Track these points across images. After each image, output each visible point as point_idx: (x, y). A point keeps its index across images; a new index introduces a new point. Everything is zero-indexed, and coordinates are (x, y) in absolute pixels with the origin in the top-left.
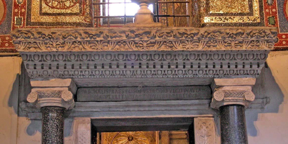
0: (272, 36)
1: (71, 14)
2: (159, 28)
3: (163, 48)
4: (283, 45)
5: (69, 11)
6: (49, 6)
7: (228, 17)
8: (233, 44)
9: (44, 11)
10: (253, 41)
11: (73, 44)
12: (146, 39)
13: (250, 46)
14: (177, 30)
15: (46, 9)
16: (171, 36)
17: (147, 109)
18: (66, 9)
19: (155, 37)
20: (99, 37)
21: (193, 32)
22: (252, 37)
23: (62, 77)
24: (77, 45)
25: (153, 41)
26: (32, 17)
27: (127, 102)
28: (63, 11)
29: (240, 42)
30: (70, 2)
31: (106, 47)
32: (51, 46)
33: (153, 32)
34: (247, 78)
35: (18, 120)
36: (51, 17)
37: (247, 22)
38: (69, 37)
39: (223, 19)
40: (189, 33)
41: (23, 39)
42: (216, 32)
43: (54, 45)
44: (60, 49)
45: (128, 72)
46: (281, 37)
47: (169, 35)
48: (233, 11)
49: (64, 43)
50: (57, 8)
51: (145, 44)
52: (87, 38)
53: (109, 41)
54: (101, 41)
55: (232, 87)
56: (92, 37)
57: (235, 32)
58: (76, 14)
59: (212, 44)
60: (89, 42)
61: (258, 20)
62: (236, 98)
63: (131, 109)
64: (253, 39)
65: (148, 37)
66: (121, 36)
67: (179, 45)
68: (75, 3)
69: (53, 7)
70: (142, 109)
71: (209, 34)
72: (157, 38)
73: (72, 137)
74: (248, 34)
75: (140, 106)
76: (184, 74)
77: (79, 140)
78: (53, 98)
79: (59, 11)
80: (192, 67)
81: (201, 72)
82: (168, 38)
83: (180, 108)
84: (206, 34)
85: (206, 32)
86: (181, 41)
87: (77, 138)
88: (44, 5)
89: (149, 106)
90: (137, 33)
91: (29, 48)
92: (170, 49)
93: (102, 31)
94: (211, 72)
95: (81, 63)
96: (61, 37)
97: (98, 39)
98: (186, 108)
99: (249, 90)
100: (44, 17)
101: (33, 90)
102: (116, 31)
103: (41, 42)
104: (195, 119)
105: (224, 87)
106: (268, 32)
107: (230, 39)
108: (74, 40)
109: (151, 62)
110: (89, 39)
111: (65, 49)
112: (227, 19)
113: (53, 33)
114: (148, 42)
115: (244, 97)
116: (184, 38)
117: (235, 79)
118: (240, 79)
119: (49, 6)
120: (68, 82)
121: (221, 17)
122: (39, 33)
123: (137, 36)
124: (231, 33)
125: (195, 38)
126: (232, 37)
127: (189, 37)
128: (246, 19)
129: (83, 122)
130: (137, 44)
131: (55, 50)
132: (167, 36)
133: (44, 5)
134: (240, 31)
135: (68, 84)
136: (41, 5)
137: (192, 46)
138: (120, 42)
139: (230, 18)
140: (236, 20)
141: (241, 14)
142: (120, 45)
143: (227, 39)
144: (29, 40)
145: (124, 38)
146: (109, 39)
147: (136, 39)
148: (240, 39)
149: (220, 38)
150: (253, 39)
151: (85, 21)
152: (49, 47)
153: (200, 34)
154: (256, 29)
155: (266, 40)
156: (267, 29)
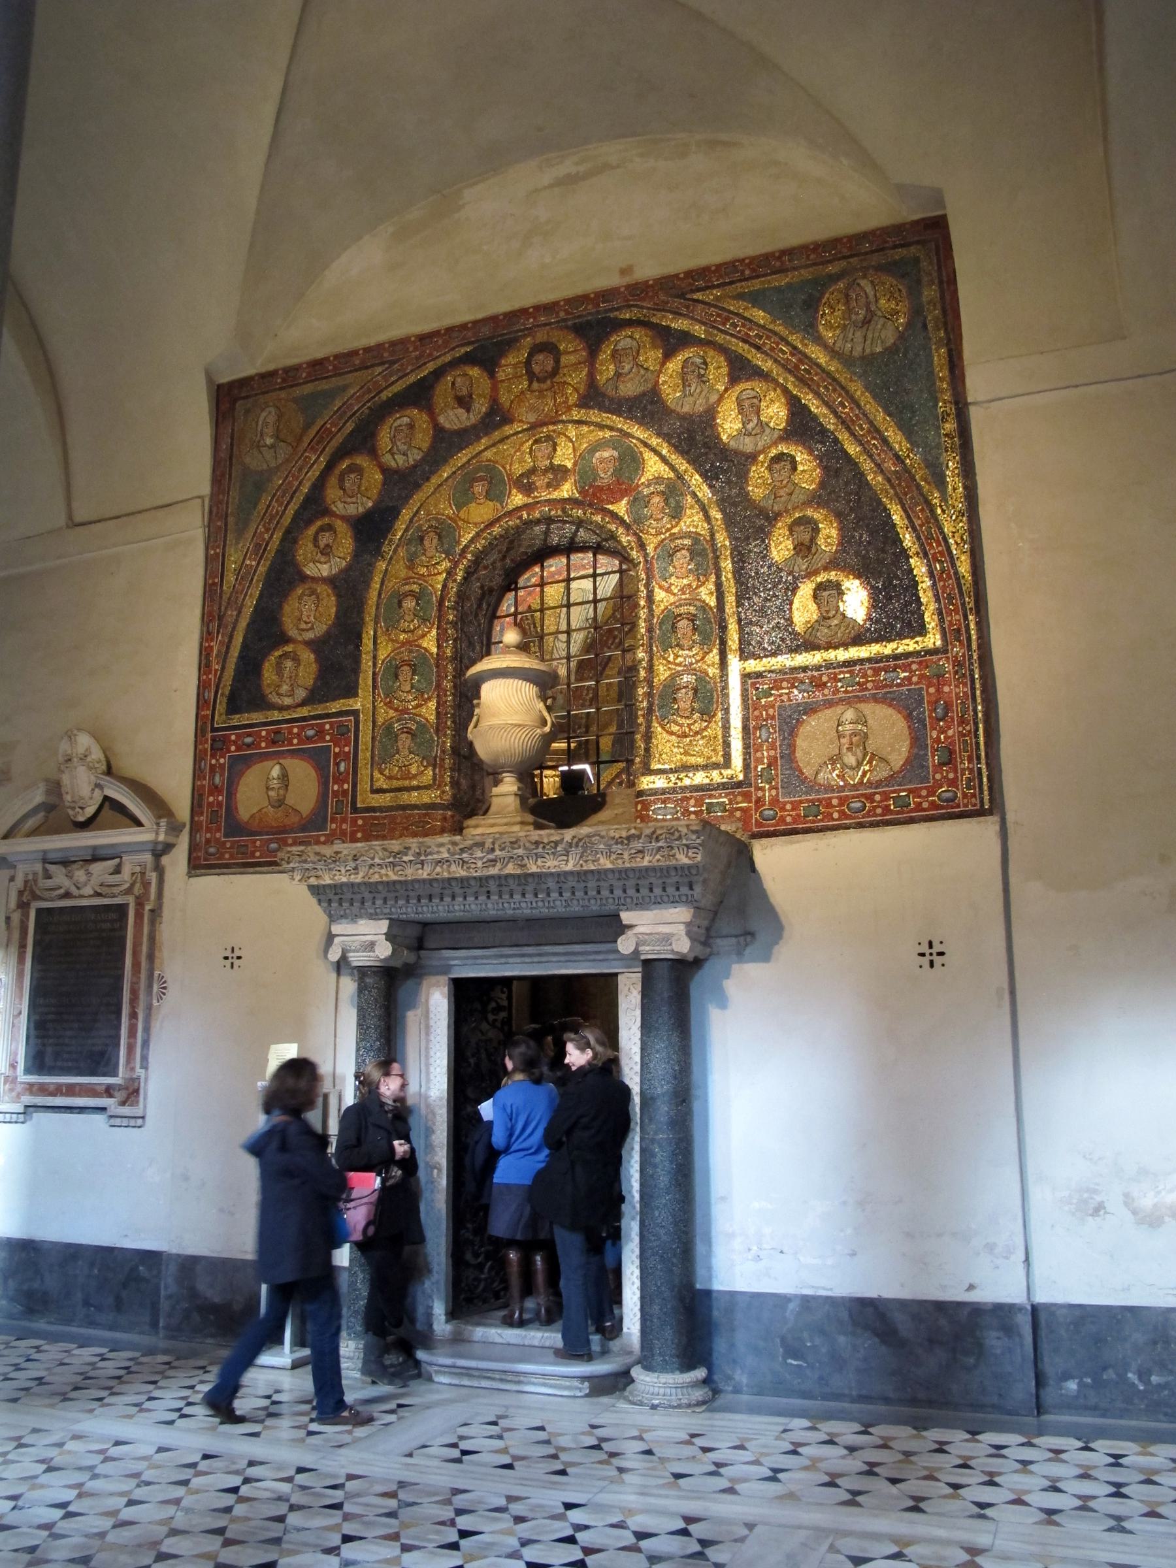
0: (694, 837)
1: (417, 788)
2: (497, 836)
3: (510, 869)
4: (787, 824)
5: (415, 783)
6: (385, 775)
7: (682, 775)
8: (626, 856)
9: (377, 785)
10: (663, 847)
11: (370, 868)
12: (479, 854)
13: (658, 857)
14: (526, 836)
15: (382, 783)
16: (519, 847)
17: (536, 959)
18: (410, 779)
19: (493, 850)
20: (406, 855)
21: (553, 839)
22: (657, 840)
23: (374, 916)
24: (376, 869)
25: (491, 856)
26: (359, 798)
27: (499, 949)
28: (406, 783)
29: (639, 852)
30: (418, 766)
31: (420, 871)
32: (338, 873)
33: (488, 845)
34: (677, 910)
35: (338, 982)
36: (388, 795)
37: (719, 781)
38: (362, 859)
39: (673, 779)
40: (546, 841)
41: (297, 865)
42: (594, 836)
43: (343, 871)
44: (353, 879)
45: (473, 907)
46: (783, 809)
47: (516, 846)
48: (692, 760)
49: (356, 868)
50: (398, 779)
51: (480, 864)
52: (389, 858)
53: (422, 861)
54: (411, 861)
55: (650, 927)
56: (395, 857)
57: (624, 834)
58: (427, 787)
59: (590, 858)
60: (394, 865)
61: (741, 777)
62: (658, 948)
63: (511, 960)
64: (660, 844)
65: (482, 852)
66: (439, 852)
67: (536, 861)
68: (426, 767)
69: (390, 778)
70: (527, 960)
71: (580, 840)
72: (498, 853)
73: (419, 1011)
74: (650, 837)
75: (523, 955)
76: (565, 907)
77: (431, 1015)
78: (364, 954)
79: (400, 783)
80: (573, 893)
81: (593, 901)
82: (515, 851)
83: (592, 957)
84: (576, 840)
85: (574, 837)
86: (536, 854)
87: (427, 1011)
88: (376, 774)
89: (540, 955)
90: (462, 846)
91: (309, 878)
92: (519, 871)
93: (407, 845)
94: (611, 901)
95: (397, 894)
96: (350, 858)
97: (405, 859)
98: (600, 957)
99: (680, 933)
100: (376, 796)
101: (336, 940)
102: (429, 844)
103: (323, 867)
104: (620, 977)
105: (637, 928)
106: (684, 830)
107: (619, 846)
108: (371, 862)
109: (505, 889)
110: (391, 860)
111: (358, 879)
112: (681, 780)
113: (337, 853)
114: (485, 860)
115: (671, 945)
116: (540, 850)
117: (655, 912)
118: (664, 911)
119: (385, 775)
120: (383, 926)
121: (671, 775)
122: (317, 854)
123: (462, 850)
124: (617, 836)
125: (559, 849)
126: (622, 843)
127: (548, 847)
128: (716, 776)
129: (437, 985)
130: (467, 863)
131: (344, 879)
132: (513, 848)
133: (376, 774)
134: (633, 831)
135: (385, 930)
136: (372, 775)
137: (556, 863)
138: (440, 862)
139: (687, 776)
140: (700, 778)
141: (705, 767)
142: (442, 867)
143: (615, 846)
144: (306, 866)
145: (446, 855)
146: (423, 858)
147: (464, 855)
148: (638, 845)
149: (602, 846)
150: (660, 844)
151: (441, 799)
152: (335, 875)
153: (565, 840)
154: (662, 827)
155: (685, 845)
156: (681, 826)
